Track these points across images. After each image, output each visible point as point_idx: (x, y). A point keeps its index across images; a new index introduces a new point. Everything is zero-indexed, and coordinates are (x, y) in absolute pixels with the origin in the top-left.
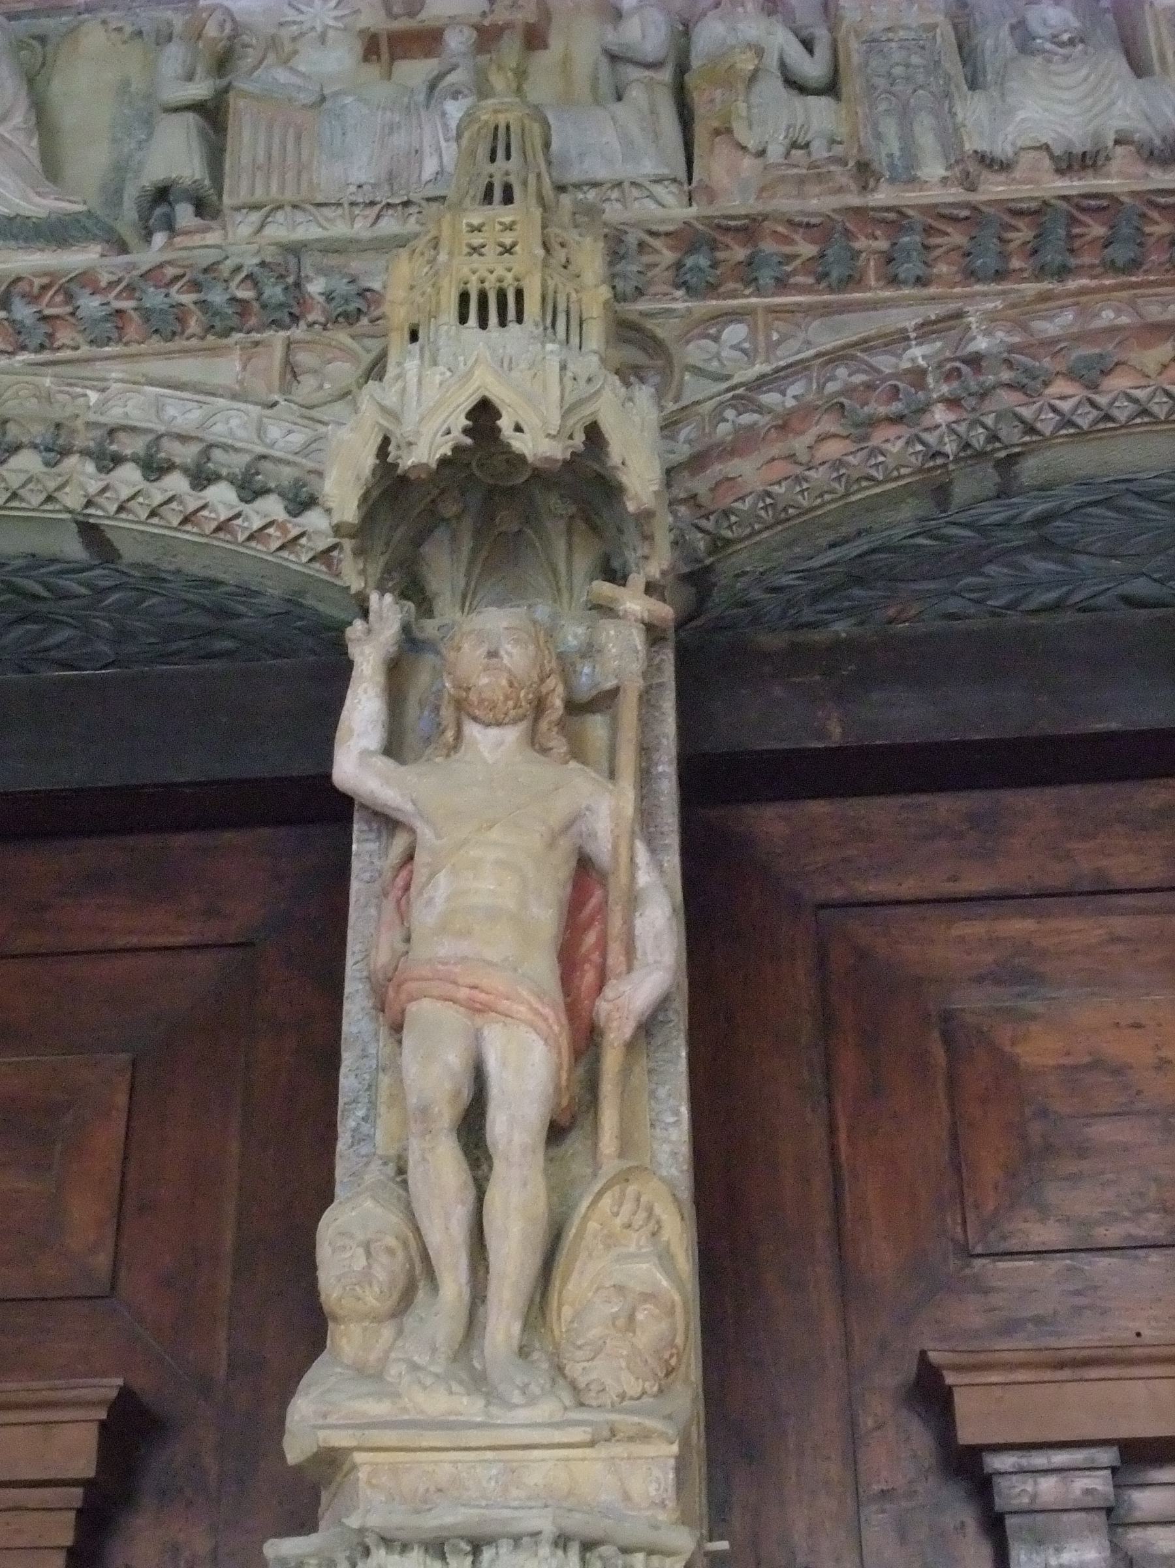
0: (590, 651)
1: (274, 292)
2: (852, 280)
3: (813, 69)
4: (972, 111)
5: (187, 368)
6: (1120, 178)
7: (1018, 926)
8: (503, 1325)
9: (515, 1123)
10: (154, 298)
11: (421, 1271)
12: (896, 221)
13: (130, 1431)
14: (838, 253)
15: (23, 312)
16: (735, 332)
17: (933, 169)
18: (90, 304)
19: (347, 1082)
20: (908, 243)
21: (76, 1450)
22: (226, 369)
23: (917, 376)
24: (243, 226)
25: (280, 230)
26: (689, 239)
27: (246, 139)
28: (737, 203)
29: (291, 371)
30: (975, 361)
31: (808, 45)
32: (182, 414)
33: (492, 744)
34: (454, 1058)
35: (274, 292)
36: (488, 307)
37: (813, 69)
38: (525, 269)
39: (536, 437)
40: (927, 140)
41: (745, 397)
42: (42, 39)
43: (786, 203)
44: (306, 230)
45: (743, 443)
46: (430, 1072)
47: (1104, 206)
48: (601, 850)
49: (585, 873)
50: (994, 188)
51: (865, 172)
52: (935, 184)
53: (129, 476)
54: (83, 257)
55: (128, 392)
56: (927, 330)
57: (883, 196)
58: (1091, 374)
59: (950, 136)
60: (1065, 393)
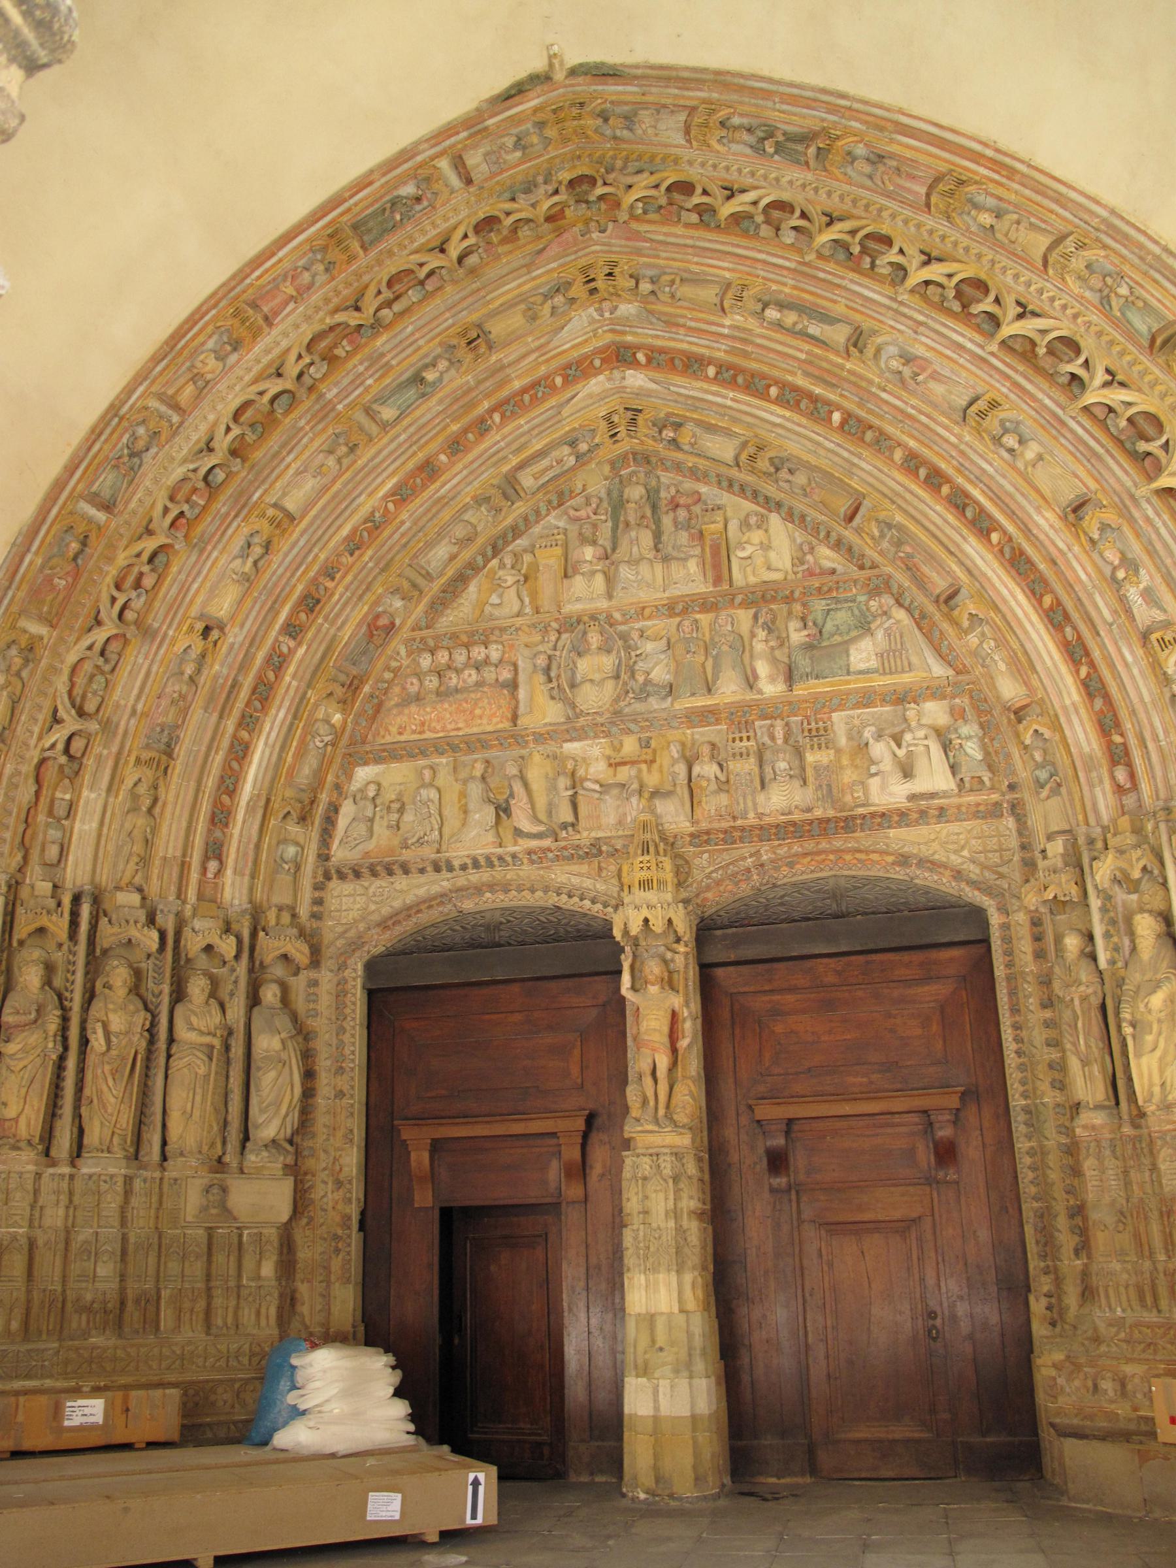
0: (673, 960)
1: (594, 851)
2: (734, 842)
3: (723, 779)
4: (761, 798)
5: (575, 868)
6: (796, 817)
7: (777, 997)
8: (662, 1112)
9: (662, 1072)
10: (566, 853)
11: (645, 1101)
12: (743, 829)
13: (590, 1119)
14: (730, 837)
15: (534, 857)
16: (706, 856)
17: (751, 815)
18: (550, 855)
19: (629, 1056)
20: (746, 834)
21: (580, 1124)
22: (584, 868)
23: (748, 870)
24: (585, 834)
25: (593, 834)
26: (692, 835)
27: (583, 810)
28: (704, 825)
29: (600, 869)
30: (762, 865)
31: (721, 766)
32: (575, 880)
33: (653, 989)
34: (650, 1061)
35: (594, 851)
36: (646, 884)
37: (723, 779)
38: (653, 874)
39: (658, 926)
40: (750, 804)
41: (708, 877)
42: (522, 758)
43: (716, 825)
44: (600, 834)
45: (708, 888)
46: (644, 1065)
47: (794, 824)
48: (677, 1008)
49: (674, 1014)
50: (767, 820)
51: (735, 818)
52: (752, 819)
53: (564, 898)
54: (547, 843)
55: (561, 875)
56: (751, 856)
57: (739, 822)
58: (791, 865)
59: (755, 804)
60: (785, 870)
